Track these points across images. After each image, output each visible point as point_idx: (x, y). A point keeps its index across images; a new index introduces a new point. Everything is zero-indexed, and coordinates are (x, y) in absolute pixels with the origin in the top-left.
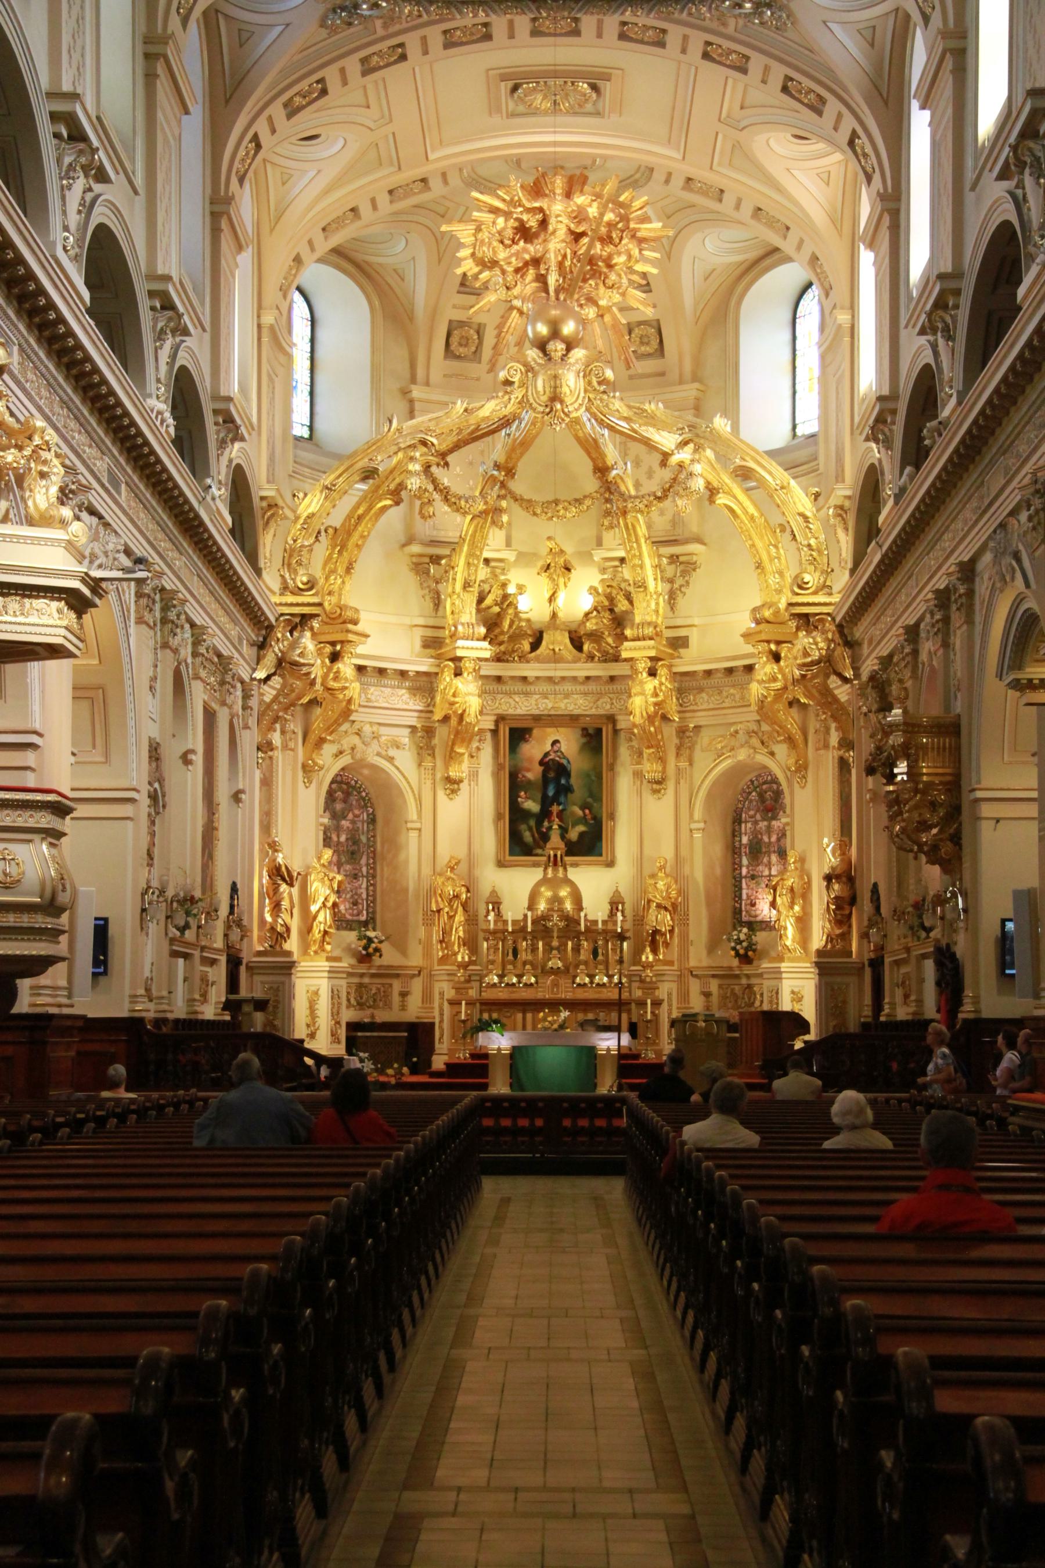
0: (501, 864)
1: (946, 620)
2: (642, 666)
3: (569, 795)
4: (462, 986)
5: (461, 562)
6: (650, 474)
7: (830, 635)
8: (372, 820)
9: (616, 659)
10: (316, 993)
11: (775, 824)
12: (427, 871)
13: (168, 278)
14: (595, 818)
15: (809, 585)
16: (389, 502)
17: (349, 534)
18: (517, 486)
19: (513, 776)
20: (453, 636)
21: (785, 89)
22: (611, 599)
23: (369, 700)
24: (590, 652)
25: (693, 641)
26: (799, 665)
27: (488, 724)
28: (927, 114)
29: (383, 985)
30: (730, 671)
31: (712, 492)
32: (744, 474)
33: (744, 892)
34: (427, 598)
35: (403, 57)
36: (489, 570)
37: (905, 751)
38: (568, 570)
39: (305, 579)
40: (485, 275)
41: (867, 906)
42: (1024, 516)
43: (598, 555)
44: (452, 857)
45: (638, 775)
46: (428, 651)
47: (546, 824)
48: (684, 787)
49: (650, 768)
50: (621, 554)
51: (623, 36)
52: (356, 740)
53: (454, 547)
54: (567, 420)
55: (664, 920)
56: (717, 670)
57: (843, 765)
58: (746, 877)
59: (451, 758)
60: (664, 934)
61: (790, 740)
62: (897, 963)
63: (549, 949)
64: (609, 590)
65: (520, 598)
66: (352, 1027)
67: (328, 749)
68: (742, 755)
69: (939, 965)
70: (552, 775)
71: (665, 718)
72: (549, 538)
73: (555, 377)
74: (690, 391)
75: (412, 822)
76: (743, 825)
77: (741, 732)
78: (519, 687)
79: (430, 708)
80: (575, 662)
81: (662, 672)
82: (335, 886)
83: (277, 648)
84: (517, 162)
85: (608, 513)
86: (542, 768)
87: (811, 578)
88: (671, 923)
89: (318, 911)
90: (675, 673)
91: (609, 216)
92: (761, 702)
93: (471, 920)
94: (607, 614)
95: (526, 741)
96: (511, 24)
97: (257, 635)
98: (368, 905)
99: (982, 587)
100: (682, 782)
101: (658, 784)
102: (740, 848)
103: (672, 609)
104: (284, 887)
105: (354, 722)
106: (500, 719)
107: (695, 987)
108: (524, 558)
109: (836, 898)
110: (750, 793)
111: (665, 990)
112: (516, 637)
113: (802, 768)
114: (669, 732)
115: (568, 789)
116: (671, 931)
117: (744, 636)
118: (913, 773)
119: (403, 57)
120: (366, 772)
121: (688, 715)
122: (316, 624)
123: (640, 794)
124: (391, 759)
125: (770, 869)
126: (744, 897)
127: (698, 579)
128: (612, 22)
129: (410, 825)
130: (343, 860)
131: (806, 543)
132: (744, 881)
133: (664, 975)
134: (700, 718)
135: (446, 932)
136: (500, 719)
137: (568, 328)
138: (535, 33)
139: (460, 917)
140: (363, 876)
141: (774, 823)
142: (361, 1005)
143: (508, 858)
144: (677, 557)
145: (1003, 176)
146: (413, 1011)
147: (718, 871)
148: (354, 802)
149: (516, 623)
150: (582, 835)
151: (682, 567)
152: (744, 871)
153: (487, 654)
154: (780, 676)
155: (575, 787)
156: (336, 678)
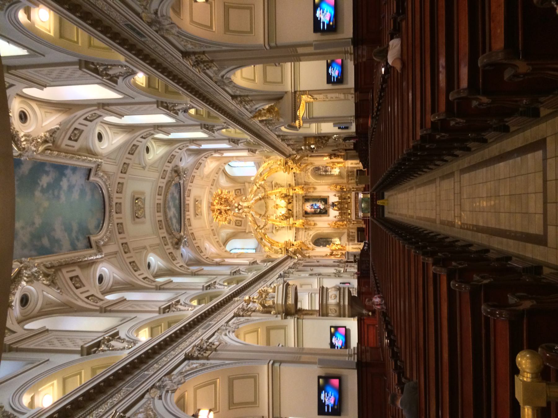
0: (329, 216)
1: (286, 139)
2: (294, 192)
5: (276, 223)
6: (261, 191)
8: (321, 238)
9: (292, 196)
11: (321, 168)
13: (231, 272)
17: (271, 243)
18: (263, 213)
21: (197, 169)
22: (282, 197)
25: (289, 183)
27: (304, 218)
28: (202, 145)
30: (295, 176)
31: (264, 180)
32: (261, 175)
35: (193, 233)
37: (309, 146)
40: (227, 220)
41: (336, 152)
42: (270, 127)
43: (274, 199)
45: (313, 192)
47: (322, 208)
48: (314, 184)
49: (311, 190)
50: (274, 196)
51: (189, 196)
53: (273, 225)
55: (338, 187)
57: (311, 156)
61: (307, 166)
62: (346, 146)
66: (358, 241)
67: (309, 246)
68: (309, 174)
69: (346, 140)
71: (303, 187)
73: (245, 207)
74: (247, 184)
81: (295, 188)
83: (292, 255)
84: (209, 214)
85: (268, 198)
87: (279, 163)
91: (218, 198)
92: (300, 171)
93: (339, 221)
96: (188, 215)
99: (281, 134)
101: (314, 188)
104: (334, 253)
106: (303, 216)
107: (350, 182)
108: (275, 212)
112: (289, 213)
113: (312, 163)
114: (305, 187)
118: (313, 144)
119: (193, 233)
122: (287, 248)
124: (311, 235)
127: (279, 182)
128: (187, 198)
134: (303, 181)
135: (341, 225)
136: (303, 216)
137: (236, 205)
138: (188, 211)
139: (338, 223)
142: (354, 240)
145: (214, 132)
146: (355, 231)
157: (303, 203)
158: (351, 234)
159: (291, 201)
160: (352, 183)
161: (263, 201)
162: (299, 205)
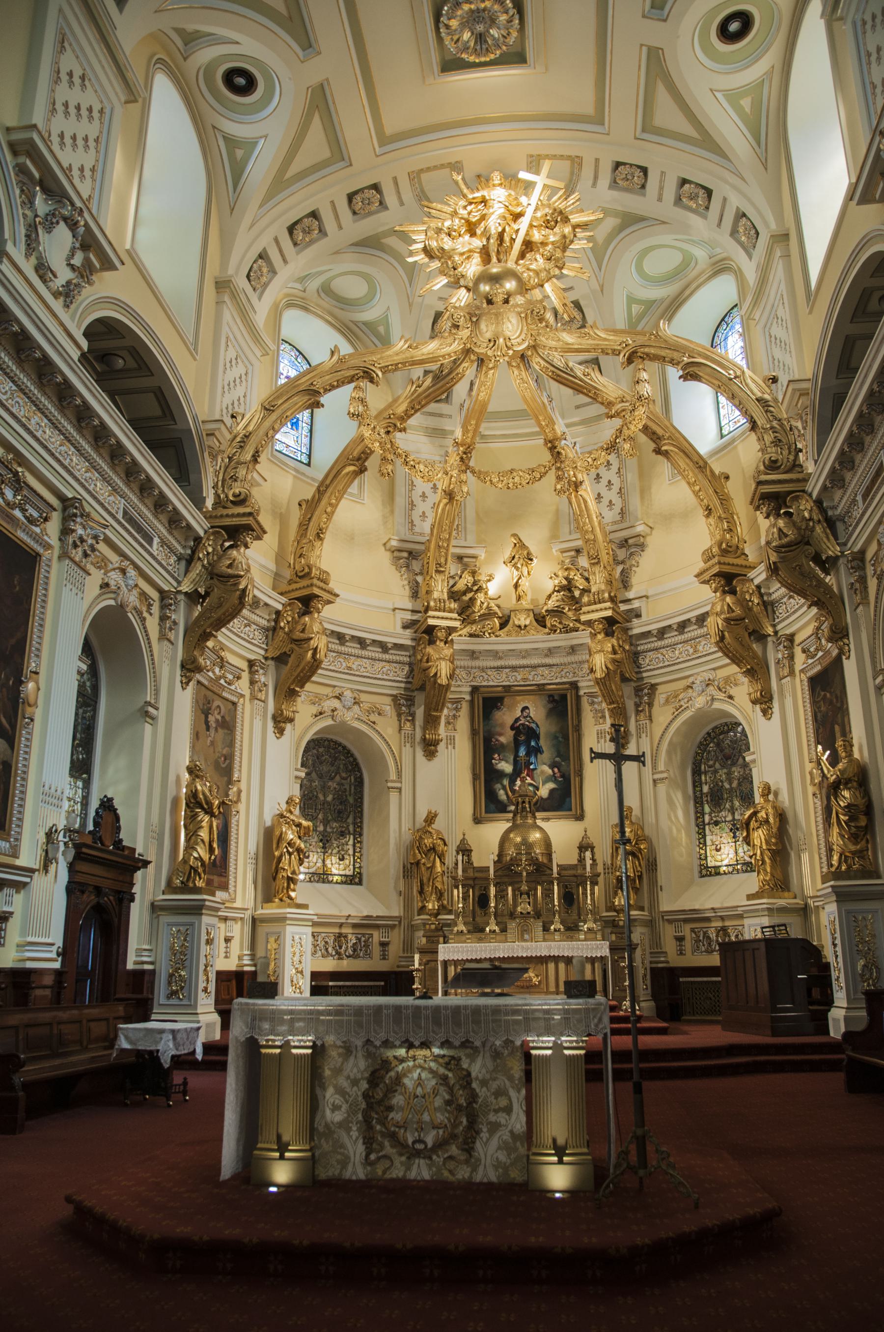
0: (477, 820)
3: (539, 755)
4: (432, 934)
7: (806, 514)
11: (737, 772)
14: (562, 776)
15: (779, 464)
16: (352, 468)
17: (319, 500)
19: (488, 740)
20: (427, 609)
23: (349, 668)
26: (776, 547)
29: (364, 935)
30: (682, 626)
33: (708, 838)
34: (407, 588)
38: (531, 560)
39: (237, 491)
40: (436, 264)
44: (430, 812)
46: (408, 630)
47: (518, 782)
52: (336, 703)
54: (511, 352)
58: (709, 824)
64: (566, 574)
65: (489, 584)
68: (700, 702)
75: (392, 781)
76: (703, 778)
79: (410, 680)
86: (512, 733)
88: (639, 869)
95: (499, 709)
97: (184, 547)
98: (355, 861)
100: (644, 735)
102: (701, 797)
105: (334, 687)
109: (849, 806)
110: (708, 745)
116: (640, 877)
117: (697, 576)
125: (733, 814)
126: (709, 843)
129: (390, 784)
130: (330, 817)
131: (768, 426)
132: (707, 827)
136: (475, 690)
140: (349, 833)
141: (734, 769)
144: (626, 541)
148: (342, 766)
149: (485, 604)
150: (552, 791)
152: (707, 818)
153: (457, 624)
155: (544, 749)
156: (303, 631)
157: (541, 687)
158: (377, 936)
160: (656, 940)
161: (546, 457)
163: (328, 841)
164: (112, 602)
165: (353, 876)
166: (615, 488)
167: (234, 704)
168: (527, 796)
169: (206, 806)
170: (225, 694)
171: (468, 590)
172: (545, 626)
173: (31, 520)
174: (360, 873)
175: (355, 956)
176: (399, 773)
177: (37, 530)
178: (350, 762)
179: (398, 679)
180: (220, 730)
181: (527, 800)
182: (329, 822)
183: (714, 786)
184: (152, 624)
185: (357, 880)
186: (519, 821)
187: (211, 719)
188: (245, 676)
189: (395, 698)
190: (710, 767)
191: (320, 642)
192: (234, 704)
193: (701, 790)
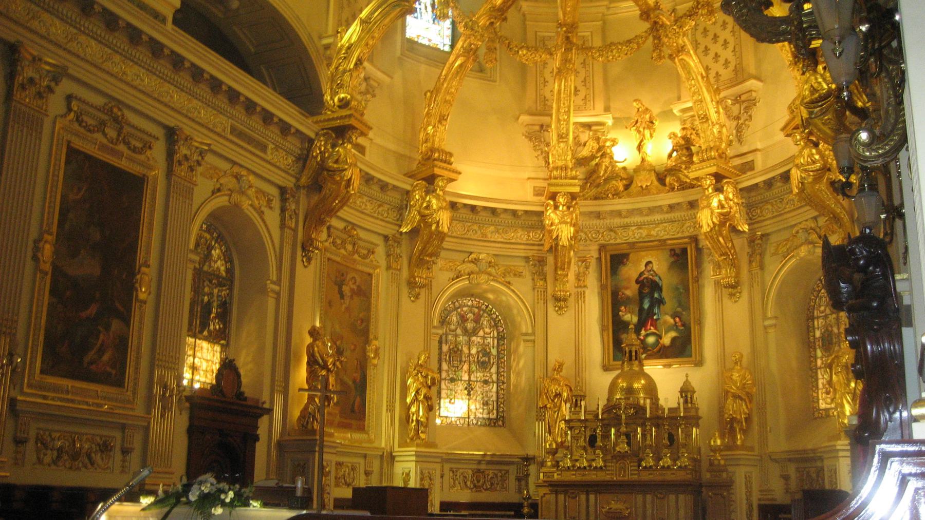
2: (708, 182)
3: (662, 306)
10: (408, 474)
12: (539, 373)
14: (683, 325)
19: (615, 294)
24: (671, 184)
29: (500, 471)
36: (591, 133)
38: (652, 122)
45: (717, 283)
47: (643, 332)
49: (727, 276)
52: (472, 267)
56: (773, 178)
59: (556, 280)
60: (740, 422)
63: (618, 435)
65: (613, 149)
70: (646, 290)
71: (734, 229)
72: (636, 100)
76: (816, 323)
77: (801, 231)
78: (617, 221)
79: (542, 242)
80: (659, 192)
81: (729, 190)
82: (429, 382)
86: (637, 286)
88: (746, 411)
89: (412, 403)
90: (741, 190)
94: (685, 151)
95: (624, 264)
100: (755, 285)
101: (733, 287)
102: (814, 342)
103: (739, 141)
107: (774, 471)
110: (820, 291)
111: (740, 475)
114: (740, 243)
115: (661, 302)
116: (748, 419)
117: (783, 129)
120: (491, 296)
121: (756, 226)
123: (720, 300)
133: (739, 459)
134: (768, 226)
136: (602, 248)
140: (493, 382)
142: (477, 488)
143: (612, 362)
147: (794, 364)
148: (485, 323)
149: (610, 168)
150: (674, 340)
151: (745, 105)
152: (819, 362)
153: (577, 189)
154: (817, 157)
155: (667, 300)
156: (427, 207)
157: (662, 243)
159: (668, 180)
162: (658, 224)
163: (472, 389)
164: (227, 204)
165: (497, 419)
166: (731, 47)
167: (370, 275)
168: (633, 345)
169: (321, 361)
170: (360, 267)
171: (593, 157)
172: (664, 184)
173: (134, 150)
174: (503, 417)
175: (492, 489)
176: (533, 327)
177: (142, 157)
178: (492, 319)
179: (531, 242)
180: (355, 297)
181: (634, 349)
182: (473, 372)
183: (824, 332)
184: (273, 217)
185: (500, 423)
186: (626, 369)
187: (346, 289)
188: (381, 251)
189: (527, 259)
190: (822, 313)
191: (444, 217)
192: (370, 275)
193: (814, 336)
